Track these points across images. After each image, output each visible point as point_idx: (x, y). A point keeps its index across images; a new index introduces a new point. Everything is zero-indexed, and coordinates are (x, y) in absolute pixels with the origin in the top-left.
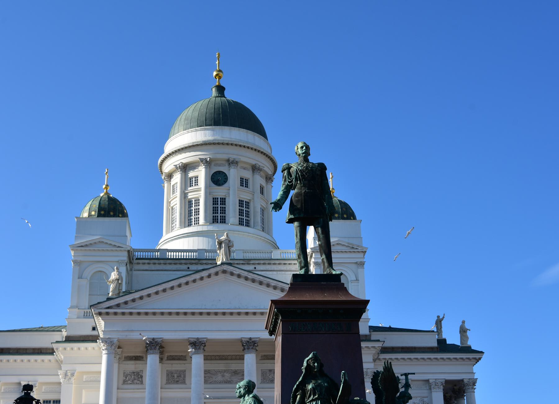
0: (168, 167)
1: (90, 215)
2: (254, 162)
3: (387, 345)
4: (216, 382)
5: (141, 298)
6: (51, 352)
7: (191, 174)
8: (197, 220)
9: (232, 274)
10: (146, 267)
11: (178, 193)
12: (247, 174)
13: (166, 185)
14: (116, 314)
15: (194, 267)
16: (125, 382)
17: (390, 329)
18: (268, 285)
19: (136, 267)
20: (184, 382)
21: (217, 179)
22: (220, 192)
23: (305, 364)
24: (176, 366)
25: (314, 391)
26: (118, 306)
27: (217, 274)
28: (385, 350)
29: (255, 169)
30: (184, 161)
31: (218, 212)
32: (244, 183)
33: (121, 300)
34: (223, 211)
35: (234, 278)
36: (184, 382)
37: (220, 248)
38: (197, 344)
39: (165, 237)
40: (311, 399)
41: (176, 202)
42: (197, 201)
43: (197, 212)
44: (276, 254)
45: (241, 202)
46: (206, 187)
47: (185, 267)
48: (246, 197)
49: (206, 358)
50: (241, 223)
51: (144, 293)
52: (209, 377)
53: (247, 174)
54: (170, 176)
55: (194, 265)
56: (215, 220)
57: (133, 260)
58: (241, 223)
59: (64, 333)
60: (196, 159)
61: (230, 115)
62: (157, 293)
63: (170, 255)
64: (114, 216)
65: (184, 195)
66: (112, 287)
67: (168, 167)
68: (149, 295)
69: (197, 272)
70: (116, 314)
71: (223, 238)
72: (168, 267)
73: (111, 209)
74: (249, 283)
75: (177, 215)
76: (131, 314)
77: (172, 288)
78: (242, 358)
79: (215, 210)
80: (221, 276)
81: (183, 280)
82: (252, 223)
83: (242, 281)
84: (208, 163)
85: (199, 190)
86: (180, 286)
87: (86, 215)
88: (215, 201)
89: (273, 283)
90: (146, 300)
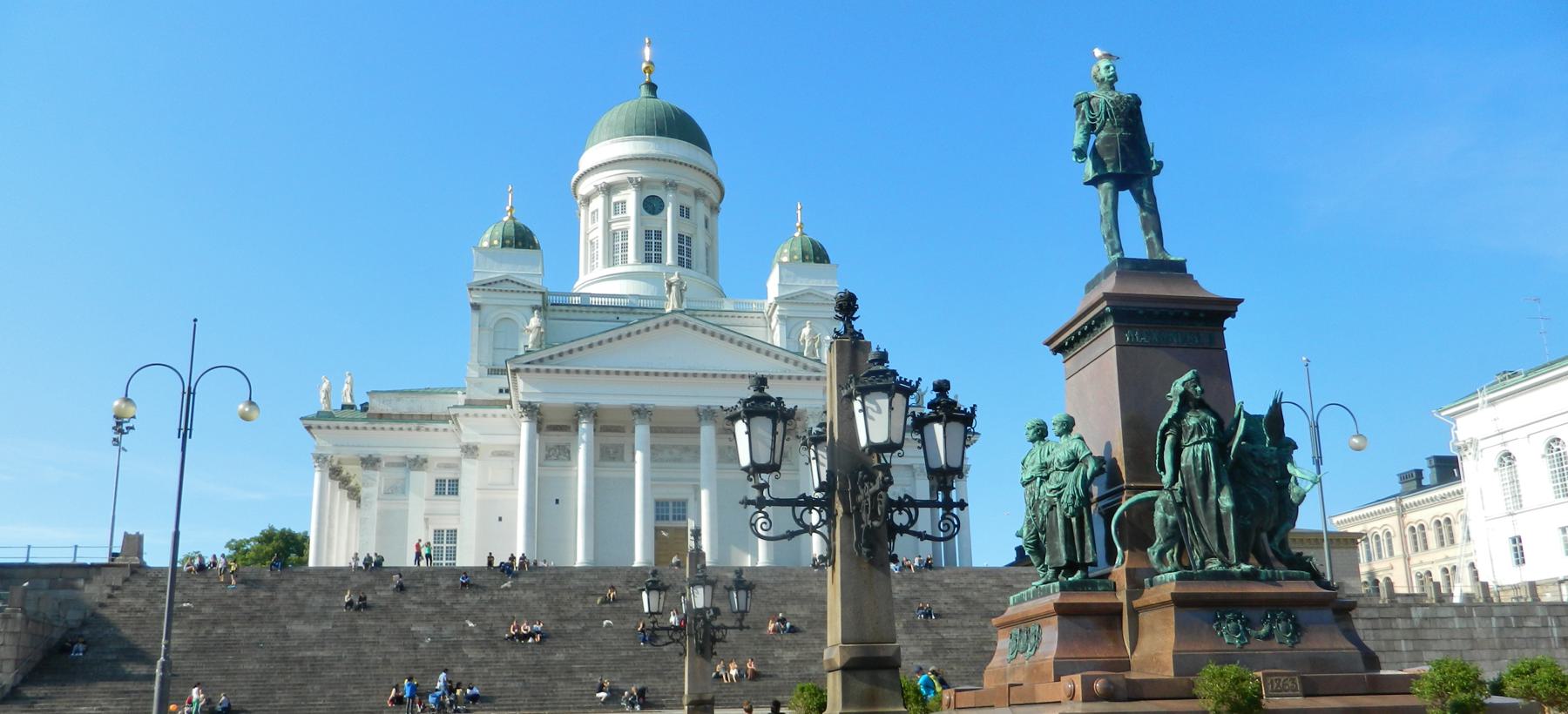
0: (585, 188)
1: (491, 245)
2: (696, 186)
4: (662, 460)
5: (571, 352)
6: (446, 419)
7: (615, 199)
8: (625, 258)
9: (686, 325)
10: (564, 315)
11: (600, 223)
12: (688, 201)
13: (583, 212)
14: (538, 371)
15: (623, 317)
16: (547, 457)
18: (731, 341)
19: (551, 315)
20: (622, 459)
21: (652, 205)
22: (653, 222)
23: (1178, 386)
24: (612, 439)
25: (1198, 429)
26: (541, 361)
27: (667, 324)
29: (699, 194)
30: (608, 181)
31: (651, 247)
32: (684, 212)
33: (545, 354)
34: (659, 247)
35: (689, 331)
36: (622, 459)
37: (670, 291)
38: (641, 412)
39: (582, 278)
40: (1195, 438)
41: (598, 234)
42: (625, 233)
43: (625, 247)
44: (728, 305)
45: (681, 237)
46: (639, 215)
47: (613, 317)
48: (686, 232)
49: (653, 430)
50: (681, 263)
51: (575, 345)
52: (655, 453)
53: (688, 201)
54: (587, 200)
55: (624, 314)
56: (648, 260)
57: (548, 306)
58: (681, 263)
59: (460, 399)
61: (678, 126)
62: (591, 346)
63: (593, 301)
64: (523, 247)
65: (607, 224)
66: (532, 336)
67: (585, 188)
68: (580, 349)
69: (628, 324)
70: (538, 371)
71: (674, 278)
72: (592, 316)
73: (521, 239)
74: (707, 337)
75: (600, 250)
76: (558, 371)
77: (610, 340)
78: (697, 431)
79: (648, 246)
80: (672, 326)
81: (613, 334)
82: (693, 264)
83: (698, 334)
84: (640, 185)
85: (627, 219)
86: (610, 340)
87: (486, 244)
88: (648, 234)
89: (739, 338)
90: (577, 354)
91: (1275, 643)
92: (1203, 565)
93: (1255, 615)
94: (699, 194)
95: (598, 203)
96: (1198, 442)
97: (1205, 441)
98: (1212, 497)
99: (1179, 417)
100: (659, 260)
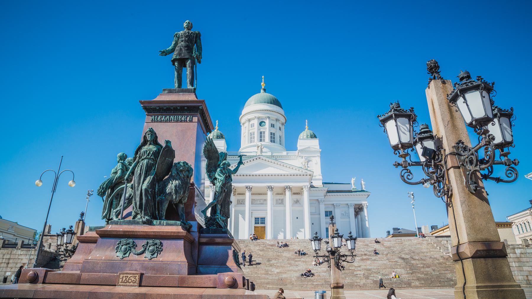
0: (243, 121)
3: (330, 189)
7: (251, 123)
12: (274, 122)
17: (332, 183)
21: (261, 124)
28: (329, 192)
29: (277, 120)
30: (249, 118)
32: (272, 126)
34: (264, 137)
42: (254, 134)
45: (271, 133)
48: (273, 132)
49: (252, 194)
54: (244, 124)
56: (261, 141)
60: (253, 117)
78: (266, 194)
79: (261, 137)
88: (261, 133)
91: (142, 257)
92: (134, 218)
93: (140, 243)
94: (277, 120)
95: (246, 125)
96: (143, 160)
97: (145, 158)
98: (141, 185)
99: (140, 148)
100: (264, 141)
